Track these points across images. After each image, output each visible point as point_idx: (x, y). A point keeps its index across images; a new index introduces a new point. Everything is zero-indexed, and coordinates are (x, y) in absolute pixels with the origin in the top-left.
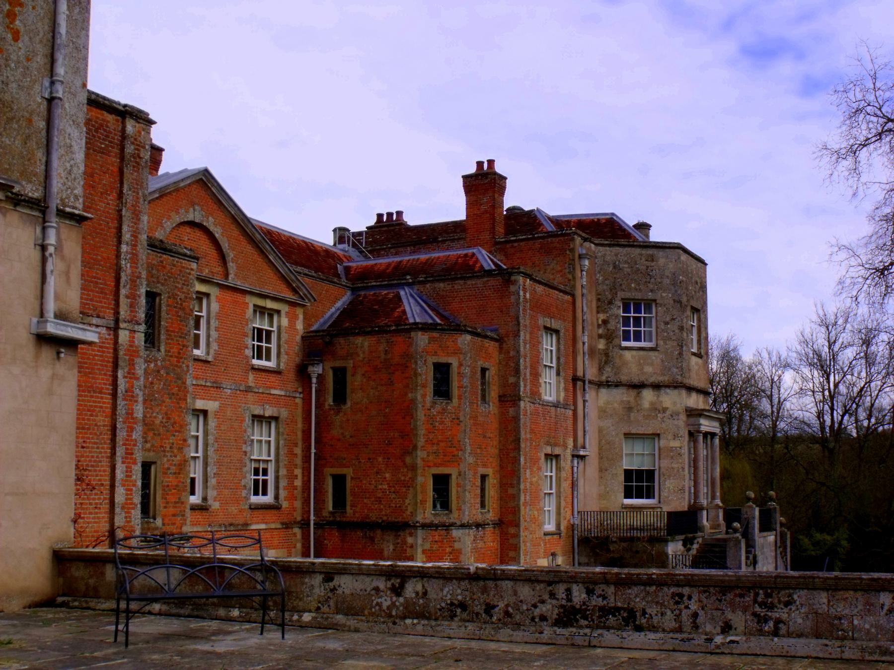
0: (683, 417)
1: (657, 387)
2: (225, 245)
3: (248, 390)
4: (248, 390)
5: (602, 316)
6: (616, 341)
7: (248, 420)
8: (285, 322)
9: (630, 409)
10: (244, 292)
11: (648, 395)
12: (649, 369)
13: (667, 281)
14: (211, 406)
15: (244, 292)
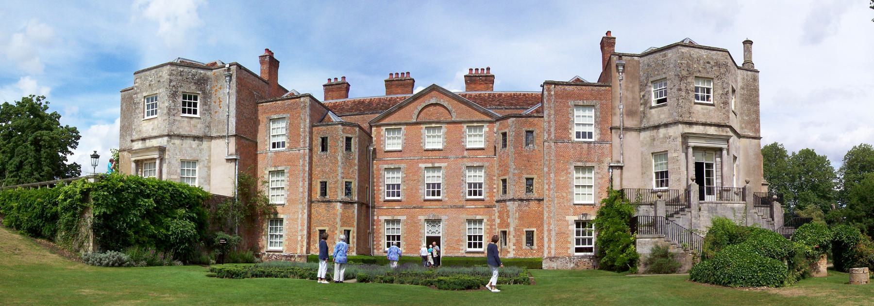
0: (680, 139)
1: (666, 125)
2: (450, 108)
3: (464, 157)
4: (464, 157)
5: (642, 94)
6: (648, 105)
7: (464, 168)
8: (487, 129)
9: (654, 140)
10: (461, 123)
11: (662, 131)
12: (662, 116)
13: (672, 66)
14: (443, 165)
15: (461, 123)
